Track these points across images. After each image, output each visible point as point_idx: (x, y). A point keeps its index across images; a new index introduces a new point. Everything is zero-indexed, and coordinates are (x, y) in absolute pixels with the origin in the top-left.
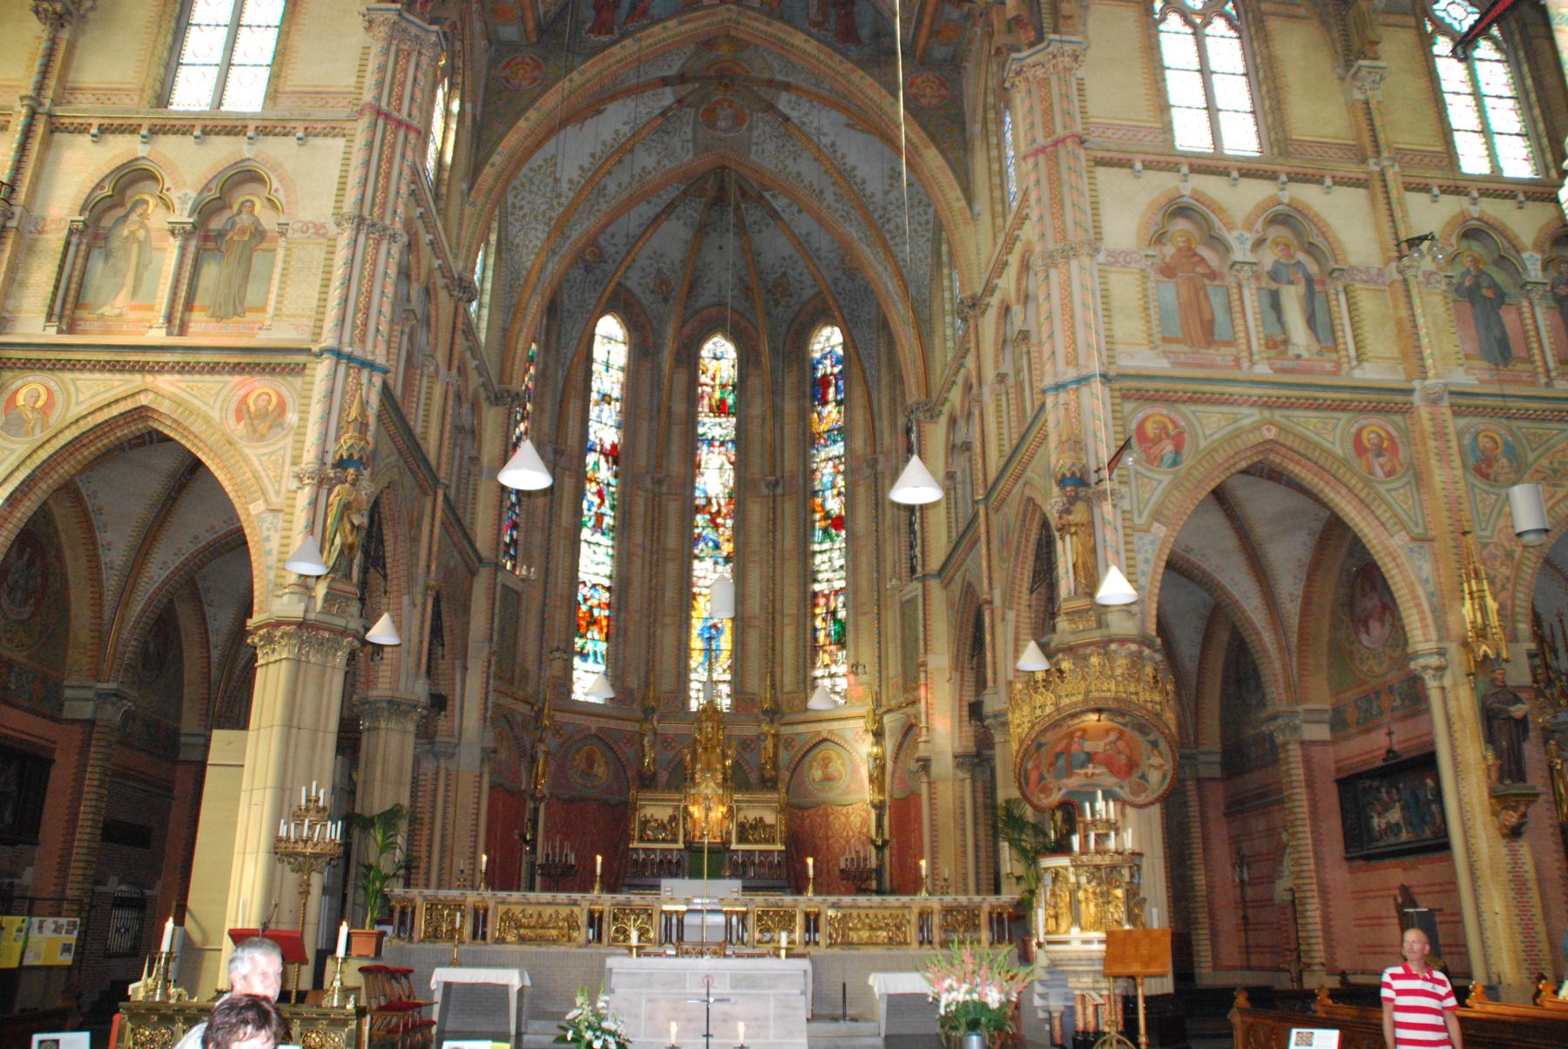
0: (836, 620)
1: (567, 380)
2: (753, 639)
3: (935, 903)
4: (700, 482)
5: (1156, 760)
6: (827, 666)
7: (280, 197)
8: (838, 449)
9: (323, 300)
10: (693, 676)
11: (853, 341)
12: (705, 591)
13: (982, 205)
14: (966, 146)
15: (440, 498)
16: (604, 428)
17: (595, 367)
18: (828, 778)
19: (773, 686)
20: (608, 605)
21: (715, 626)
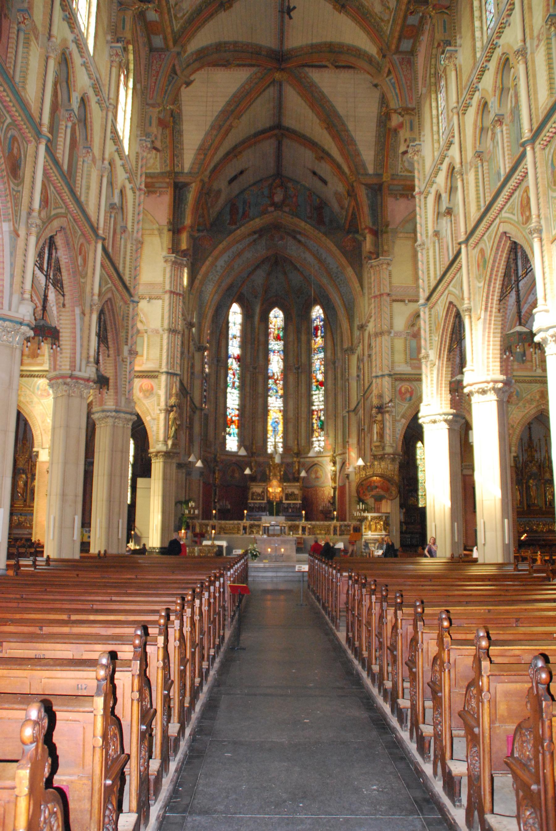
0: (321, 421)
1: (221, 333)
2: (290, 426)
3: (338, 524)
4: (270, 367)
5: (393, 488)
7: (144, 319)
8: (322, 355)
9: (161, 355)
10: (269, 440)
12: (272, 408)
13: (366, 291)
14: (361, 266)
15: (188, 398)
16: (234, 349)
17: (230, 325)
18: (317, 478)
19: (298, 444)
20: (238, 416)
21: (276, 422)
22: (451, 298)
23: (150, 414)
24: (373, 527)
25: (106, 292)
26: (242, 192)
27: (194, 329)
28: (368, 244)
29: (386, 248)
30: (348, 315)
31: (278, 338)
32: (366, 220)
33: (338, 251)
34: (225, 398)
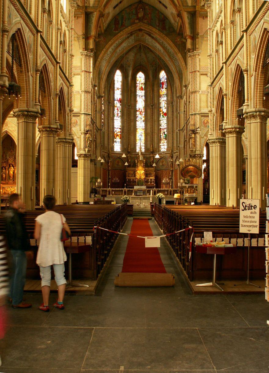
0: (165, 134)
4: (137, 105)
6: (163, 143)
8: (165, 99)
9: (81, 105)
10: (137, 145)
11: (168, 78)
15: (95, 125)
16: (118, 95)
19: (153, 147)
22: (221, 86)
23: (76, 135)
24: (189, 191)
25: (43, 60)
26: (121, 12)
27: (96, 88)
28: (189, 45)
29: (197, 46)
30: (179, 77)
32: (188, 32)
33: (173, 45)
34: (113, 122)
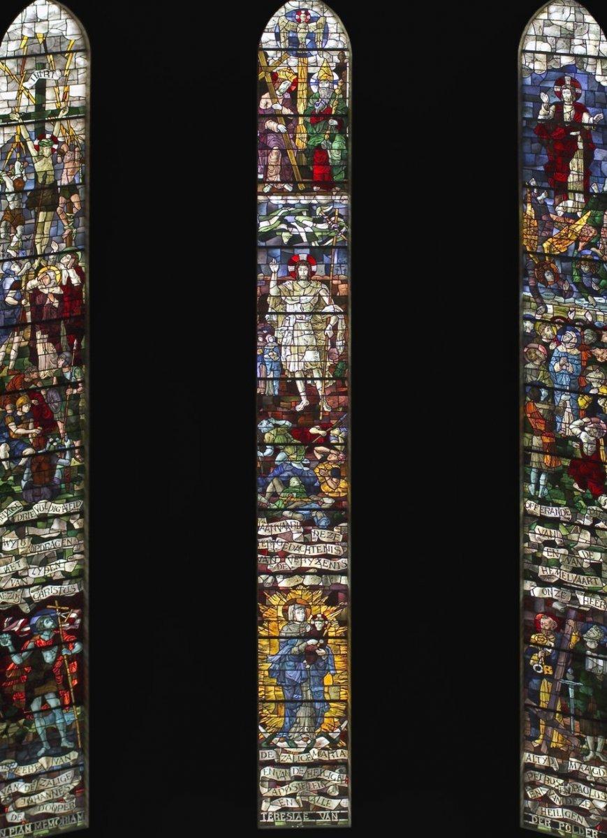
21: (309, 654)
31: (312, 173)
